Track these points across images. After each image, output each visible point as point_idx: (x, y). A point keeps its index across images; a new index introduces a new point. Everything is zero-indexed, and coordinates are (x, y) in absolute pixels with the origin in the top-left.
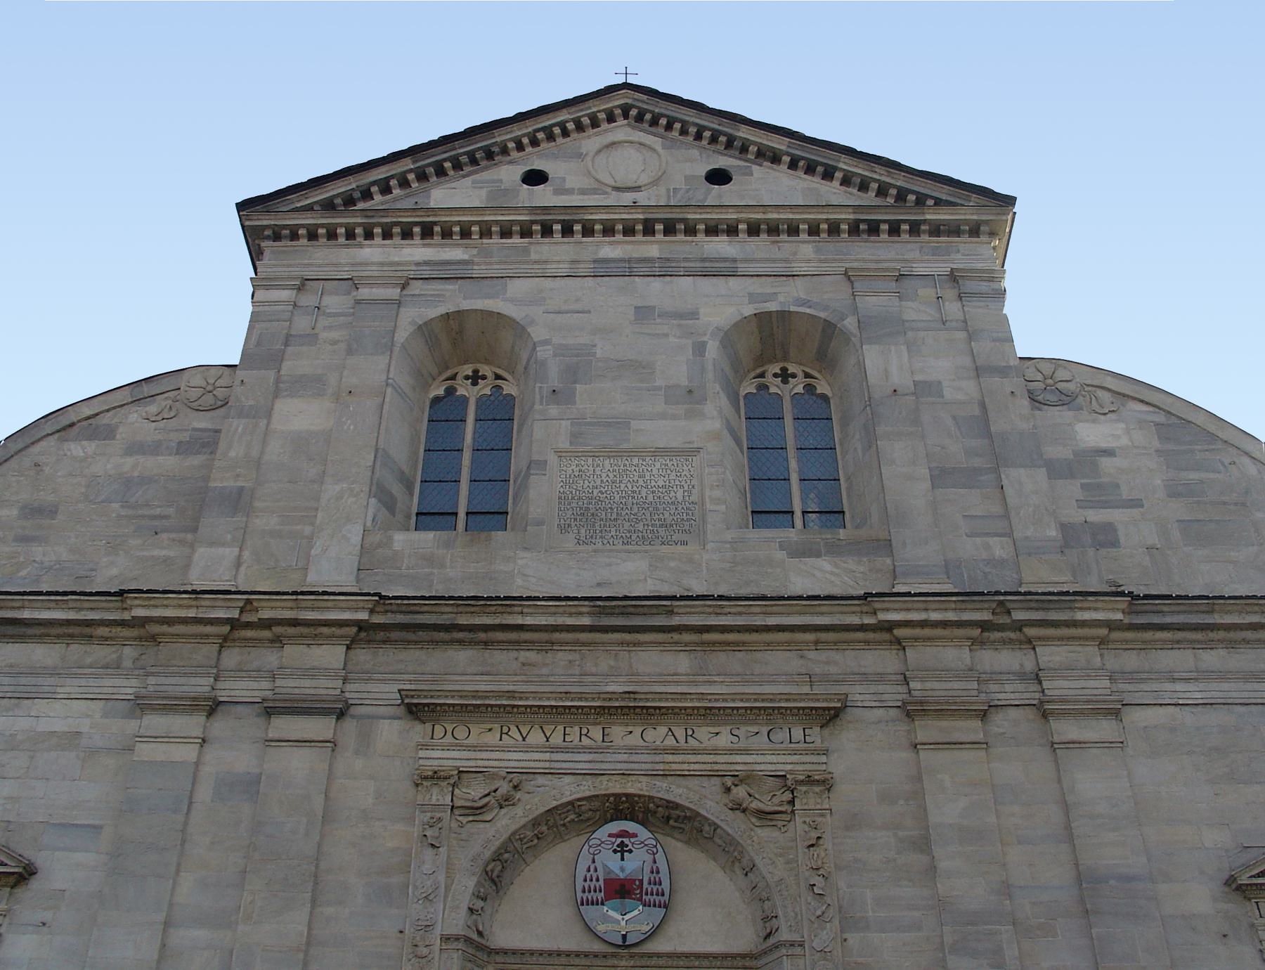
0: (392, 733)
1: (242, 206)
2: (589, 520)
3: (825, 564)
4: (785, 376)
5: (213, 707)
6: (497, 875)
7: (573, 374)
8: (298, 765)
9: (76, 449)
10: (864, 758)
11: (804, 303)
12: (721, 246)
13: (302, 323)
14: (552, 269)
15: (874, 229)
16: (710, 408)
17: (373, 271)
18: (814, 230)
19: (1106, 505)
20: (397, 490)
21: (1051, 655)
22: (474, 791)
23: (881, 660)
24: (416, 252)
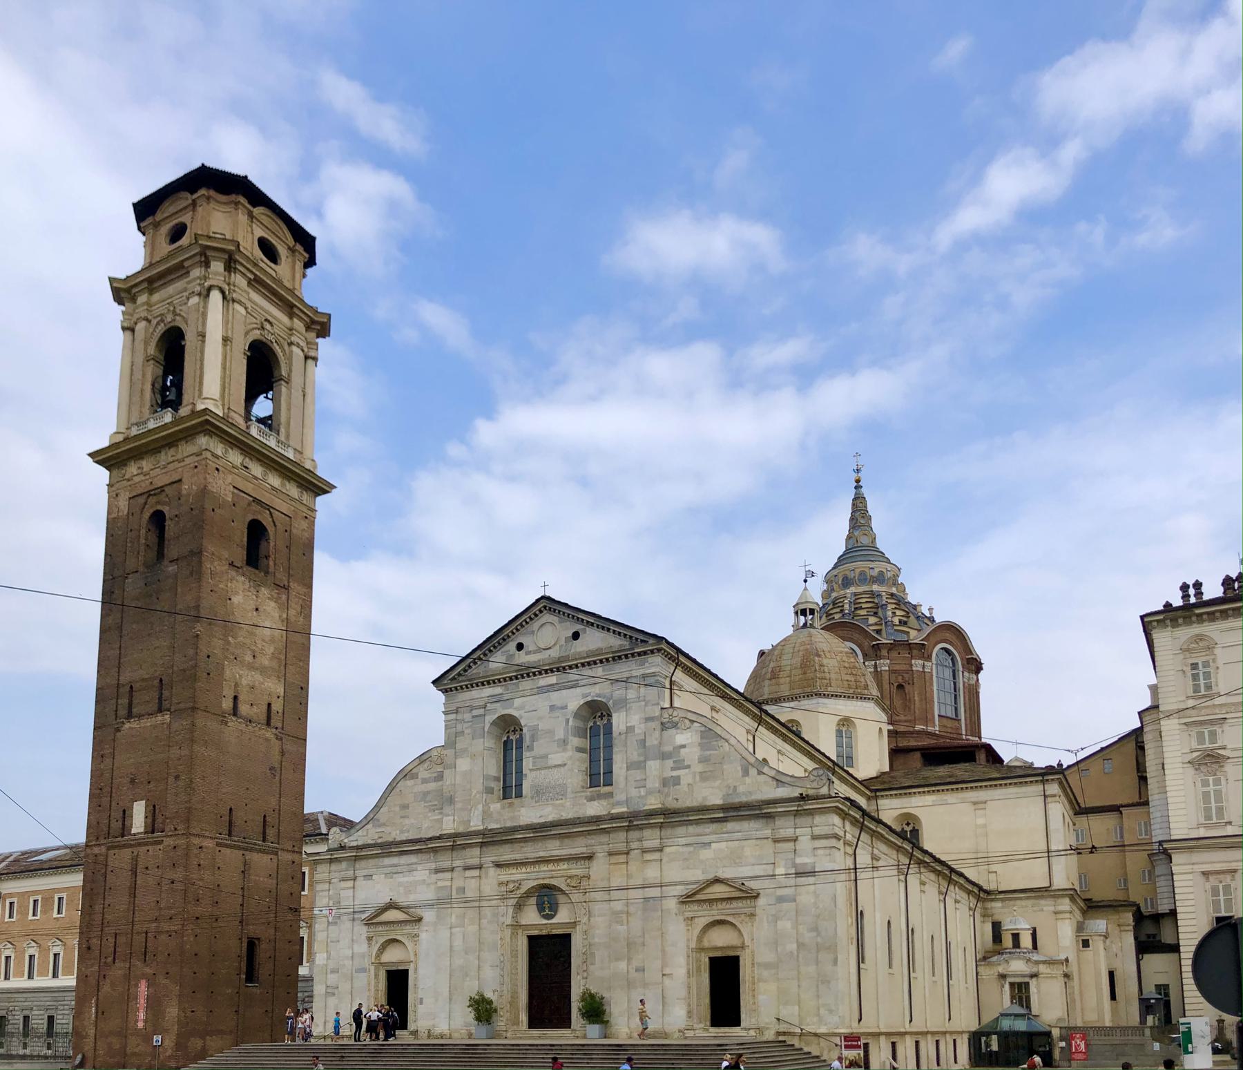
0: (492, 871)
1: (434, 682)
2: (538, 792)
3: (596, 803)
4: (602, 716)
5: (452, 870)
6: (519, 907)
7: (533, 738)
8: (473, 884)
9: (410, 783)
10: (599, 869)
11: (599, 696)
12: (573, 675)
13: (459, 727)
14: (526, 693)
15: (620, 657)
16: (569, 747)
17: (476, 703)
18: (601, 661)
19: (679, 769)
20: (493, 784)
21: (647, 833)
22: (511, 886)
23: (604, 838)
24: (488, 691)
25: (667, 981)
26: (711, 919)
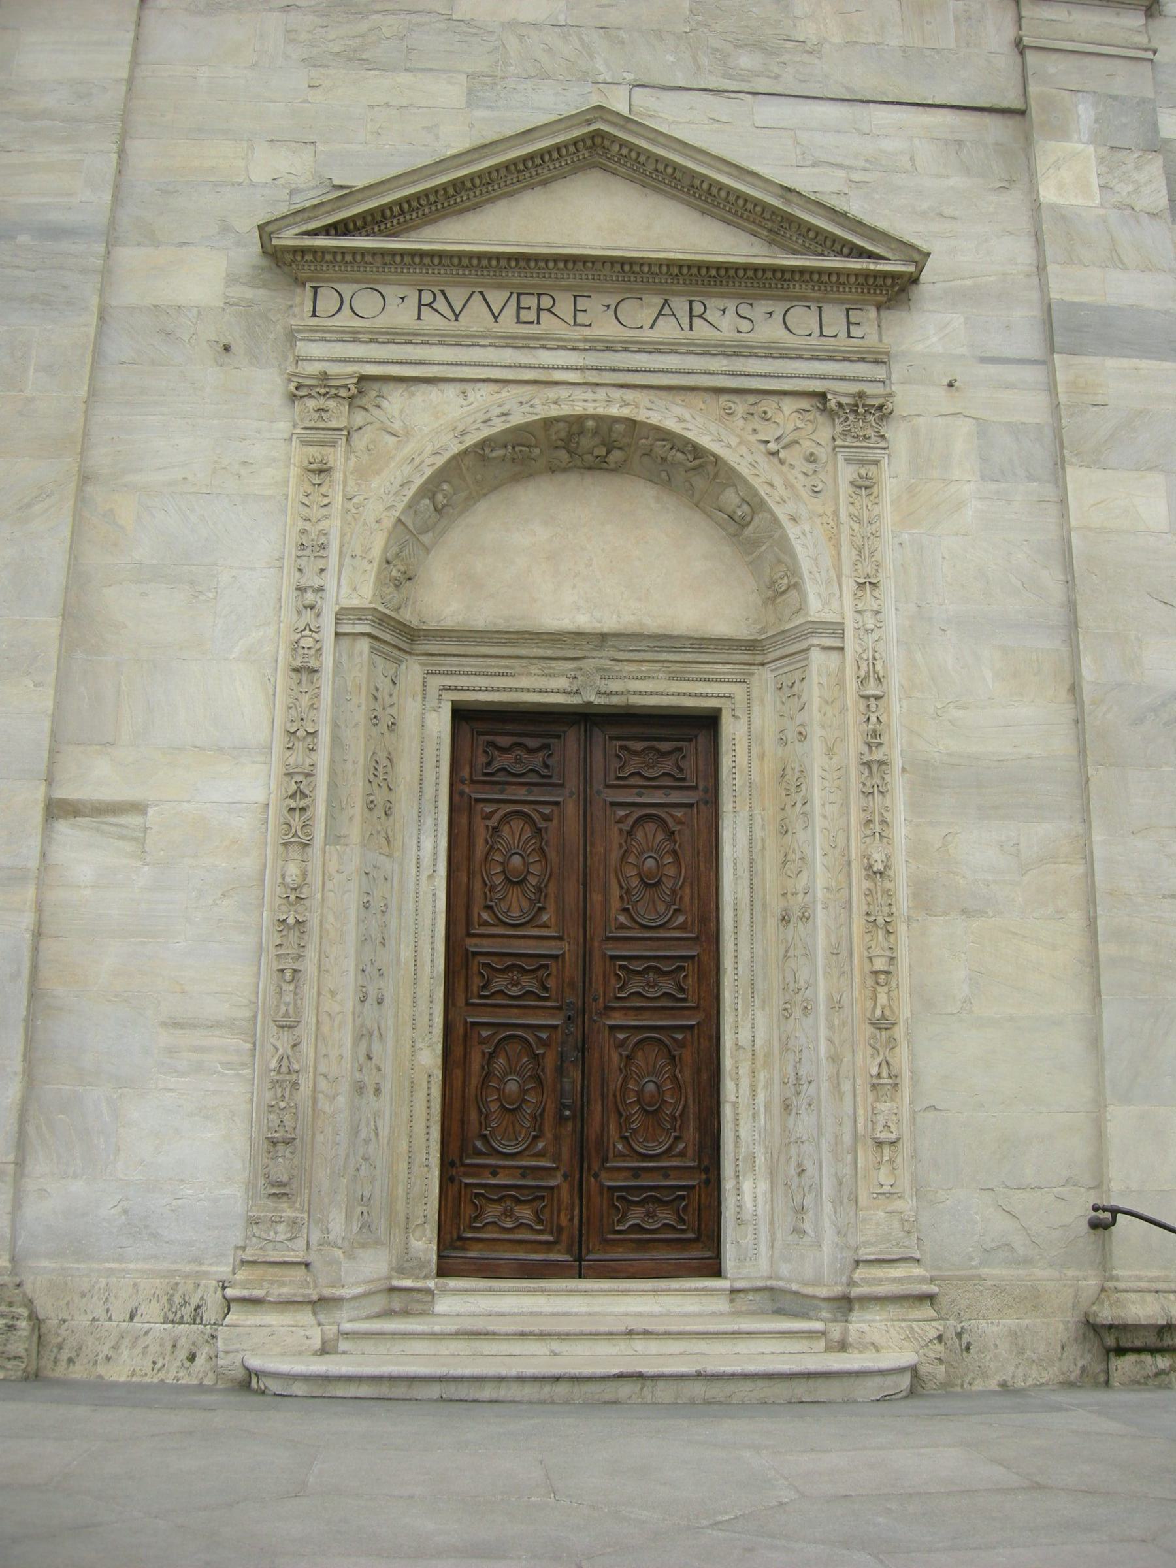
25: (82, 854)
26: (524, 408)
